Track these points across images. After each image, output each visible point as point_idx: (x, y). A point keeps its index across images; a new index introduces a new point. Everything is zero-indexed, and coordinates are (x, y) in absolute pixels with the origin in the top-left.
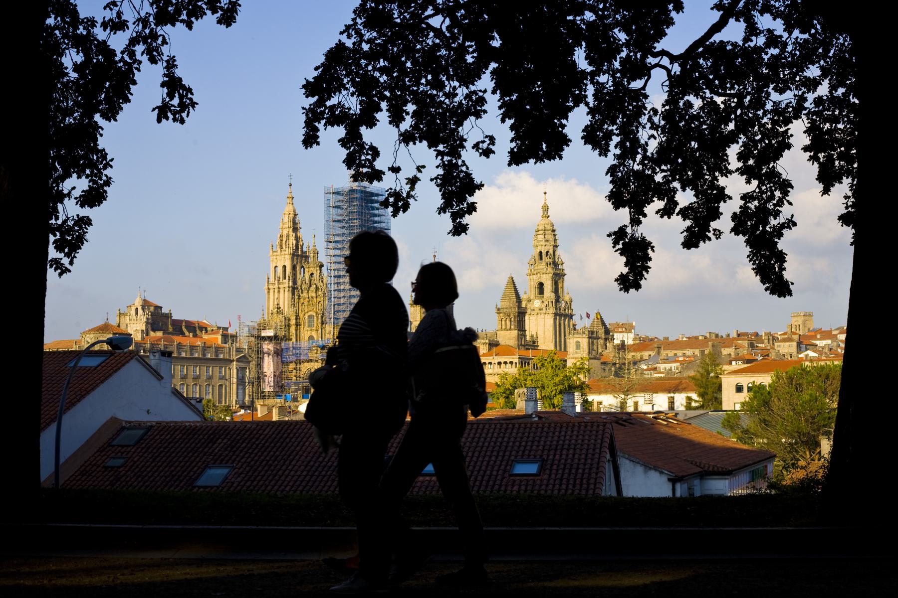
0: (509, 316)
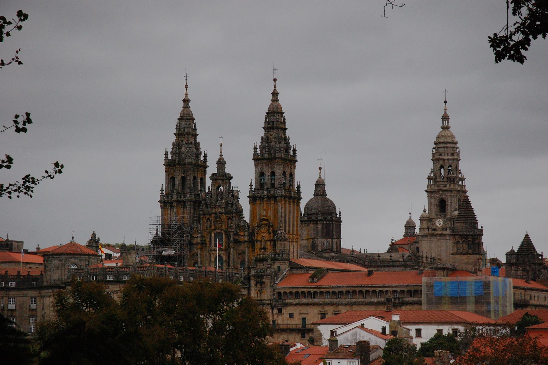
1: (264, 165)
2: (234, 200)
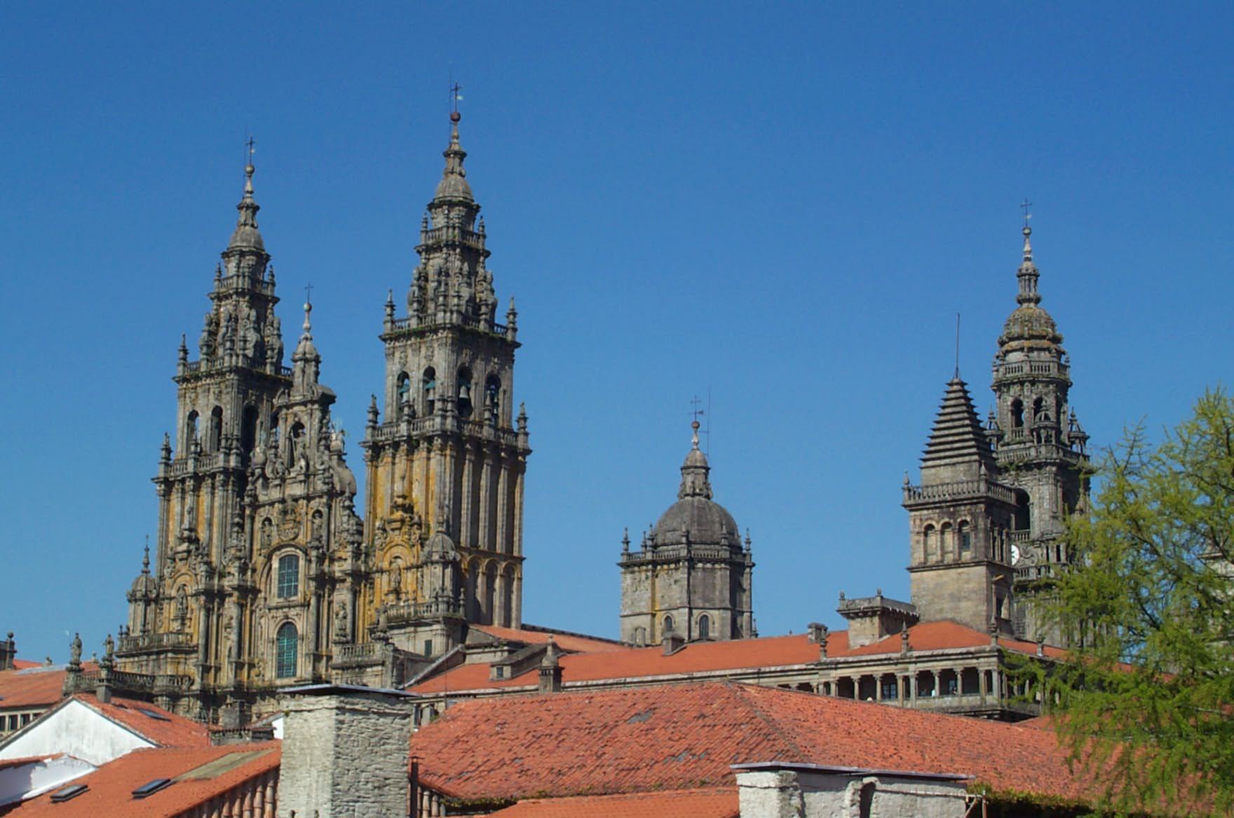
0: (952, 515)
1: (410, 351)
2: (330, 459)
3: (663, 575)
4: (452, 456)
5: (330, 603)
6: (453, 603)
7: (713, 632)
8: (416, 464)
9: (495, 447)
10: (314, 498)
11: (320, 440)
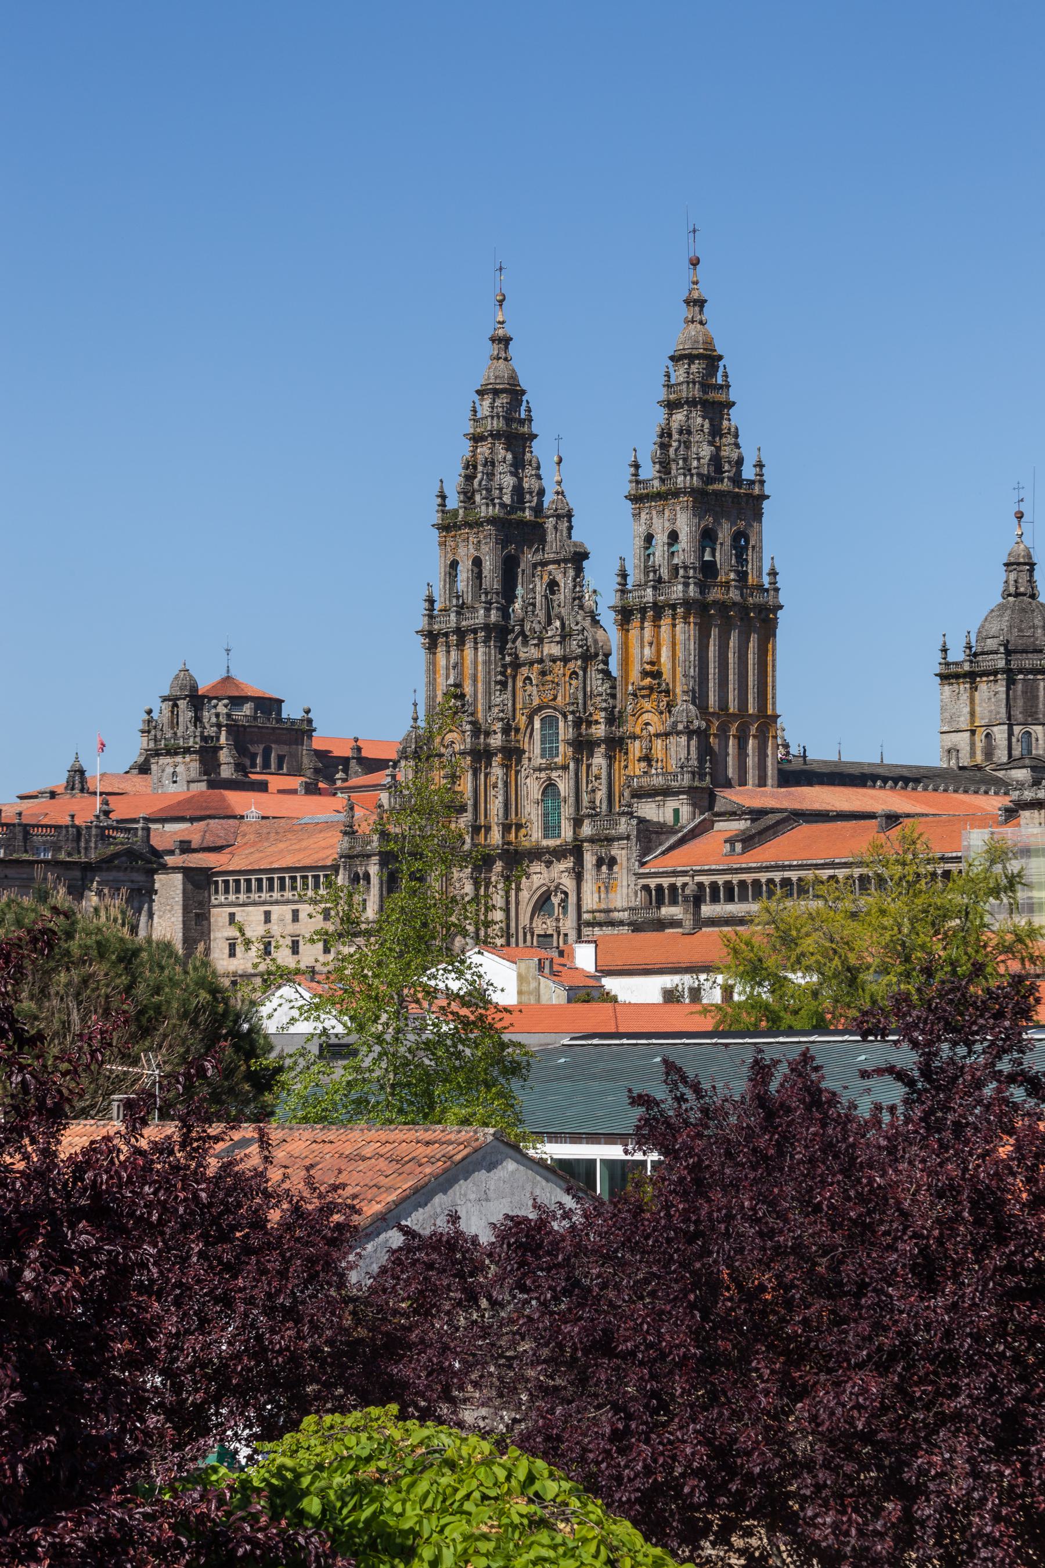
3: (983, 687)
4: (695, 624)
5: (589, 766)
6: (699, 773)
7: (1037, 748)
8: (663, 629)
9: (743, 609)
10: (570, 660)
11: (574, 599)
